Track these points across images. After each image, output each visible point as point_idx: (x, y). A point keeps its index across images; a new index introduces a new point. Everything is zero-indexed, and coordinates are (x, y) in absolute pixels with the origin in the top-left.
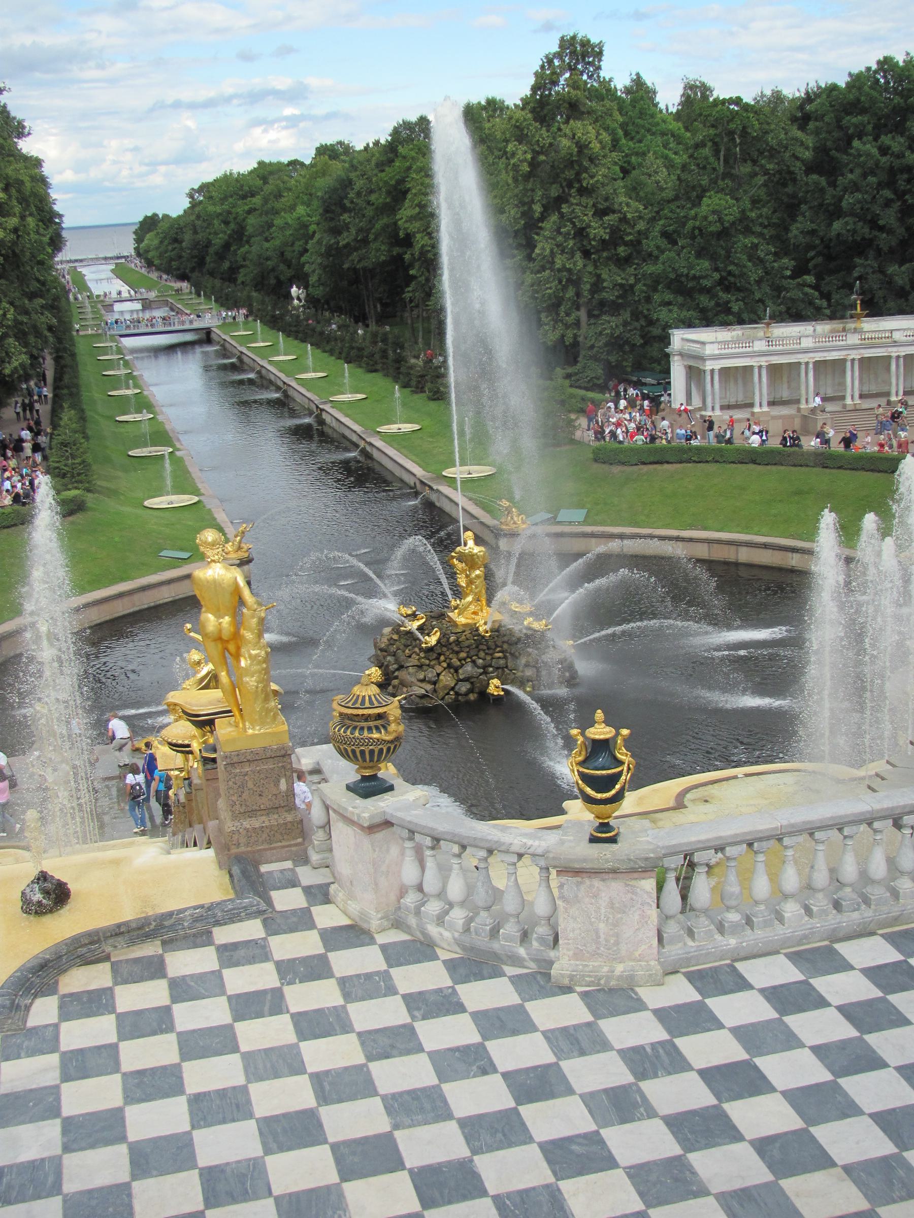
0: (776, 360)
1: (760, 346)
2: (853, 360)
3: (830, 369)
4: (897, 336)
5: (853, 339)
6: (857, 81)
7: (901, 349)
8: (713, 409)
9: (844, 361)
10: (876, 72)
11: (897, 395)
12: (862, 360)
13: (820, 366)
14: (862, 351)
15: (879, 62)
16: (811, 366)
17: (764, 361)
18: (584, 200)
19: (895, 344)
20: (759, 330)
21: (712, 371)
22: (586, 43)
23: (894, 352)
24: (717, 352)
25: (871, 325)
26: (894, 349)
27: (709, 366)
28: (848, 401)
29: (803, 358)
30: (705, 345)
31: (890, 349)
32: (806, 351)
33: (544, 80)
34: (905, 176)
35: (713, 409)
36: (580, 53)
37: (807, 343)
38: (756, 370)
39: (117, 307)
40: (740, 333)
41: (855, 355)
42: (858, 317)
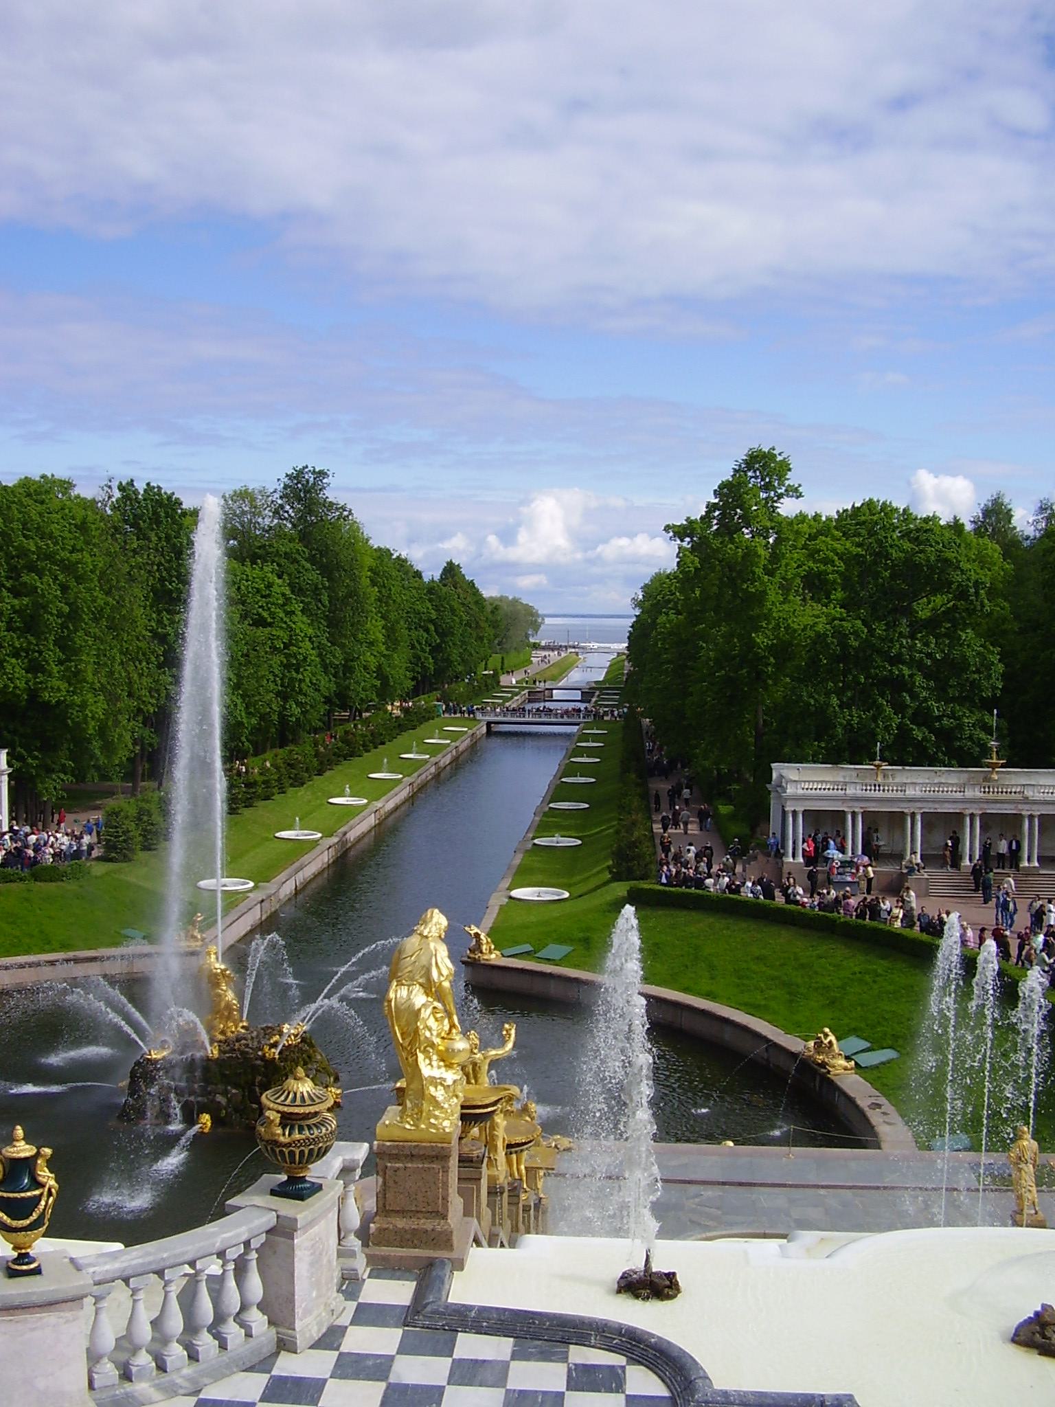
0: (873, 808)
2: (972, 816)
3: (944, 825)
4: (1029, 793)
7: (1035, 807)
11: (1029, 860)
12: (982, 816)
13: (931, 821)
14: (985, 806)
16: (919, 817)
19: (1026, 801)
21: (795, 813)
24: (800, 792)
26: (1027, 807)
31: (1020, 807)
38: (849, 817)
42: (993, 766)
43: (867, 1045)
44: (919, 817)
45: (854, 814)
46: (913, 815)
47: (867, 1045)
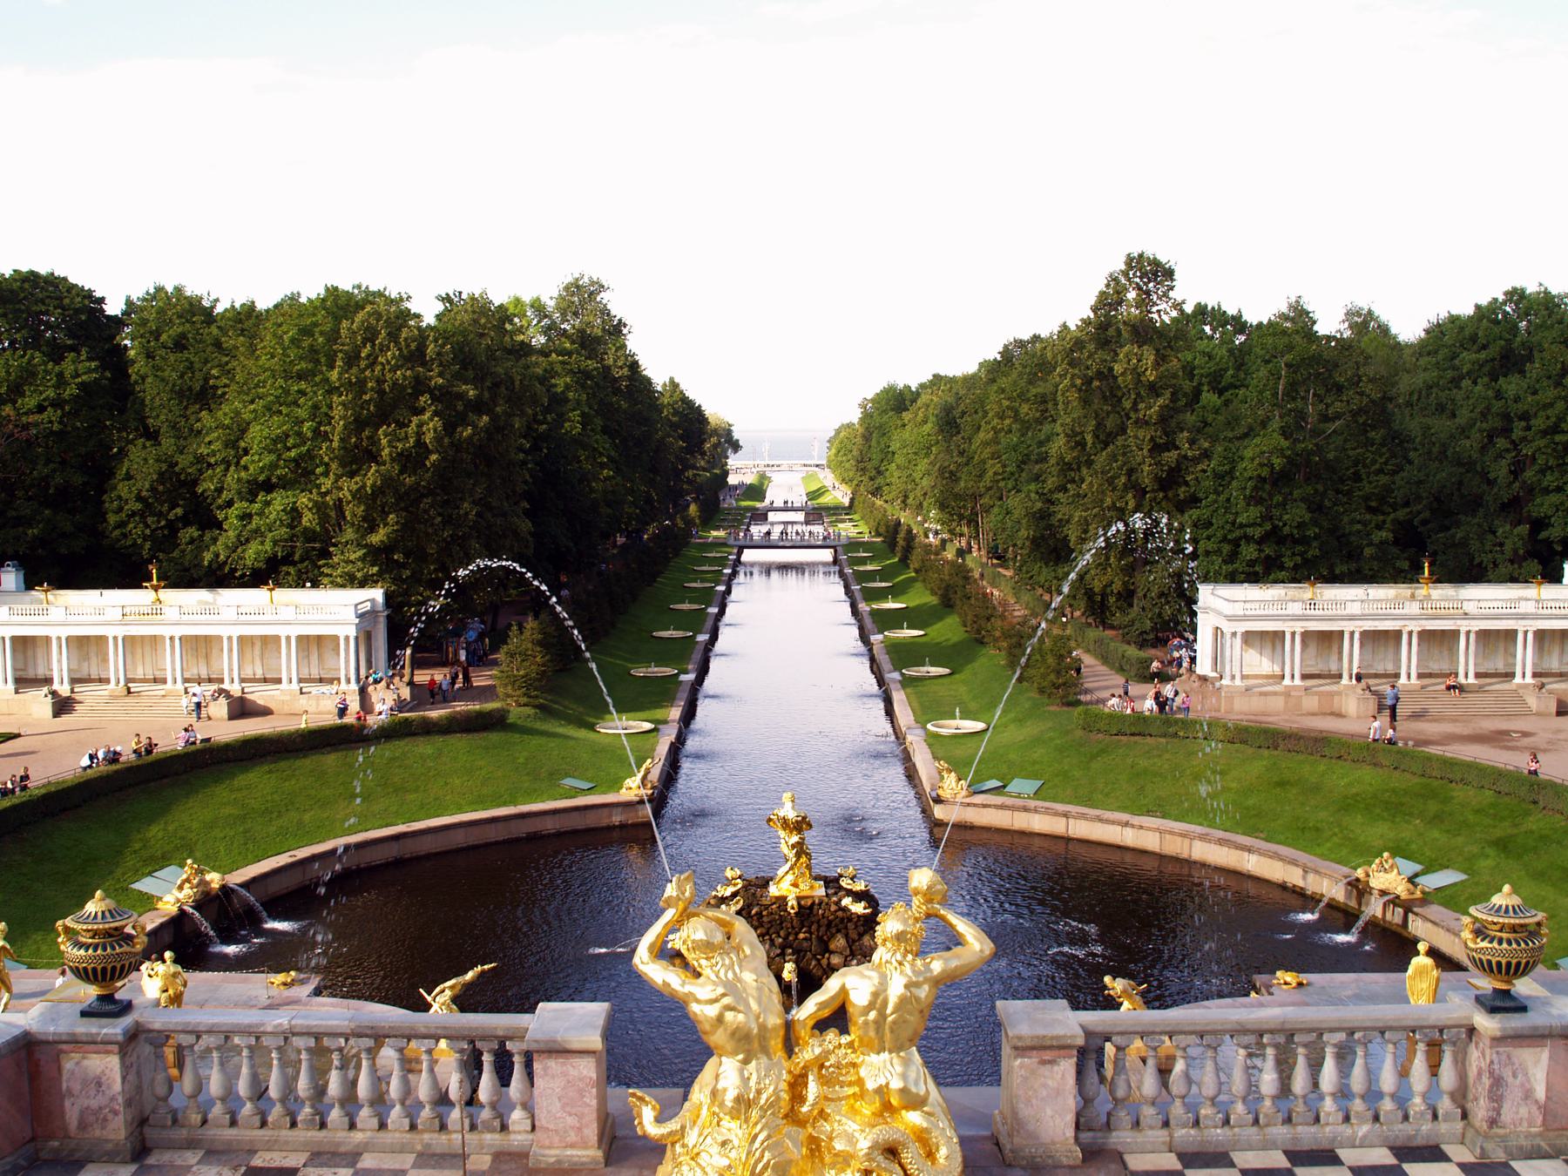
1: (1295, 609)
4: (1470, 607)
5: (1413, 608)
6: (1485, 314)
8: (1233, 677)
9: (1398, 634)
10: (1504, 303)
14: (1423, 622)
15: (1506, 294)
16: (1357, 636)
17: (1299, 627)
18: (1141, 434)
20: (1305, 592)
21: (1234, 634)
22: (1156, 263)
23: (1463, 626)
25: (1442, 593)
27: (1227, 628)
28: (1403, 680)
29: (1347, 627)
30: (1222, 607)
32: (1352, 618)
33: (1108, 302)
34: (1523, 424)
35: (1233, 677)
36: (1152, 273)
37: (1355, 609)
39: (772, 516)
40: (1282, 592)
41: (1416, 627)
43: (1418, 868)
44: (1357, 636)
45: (1293, 634)
46: (1352, 633)
47: (1418, 868)
